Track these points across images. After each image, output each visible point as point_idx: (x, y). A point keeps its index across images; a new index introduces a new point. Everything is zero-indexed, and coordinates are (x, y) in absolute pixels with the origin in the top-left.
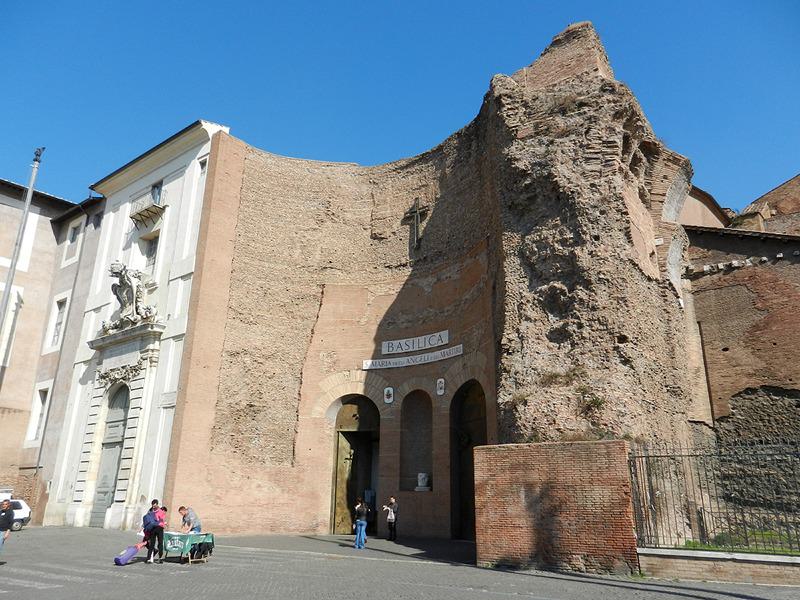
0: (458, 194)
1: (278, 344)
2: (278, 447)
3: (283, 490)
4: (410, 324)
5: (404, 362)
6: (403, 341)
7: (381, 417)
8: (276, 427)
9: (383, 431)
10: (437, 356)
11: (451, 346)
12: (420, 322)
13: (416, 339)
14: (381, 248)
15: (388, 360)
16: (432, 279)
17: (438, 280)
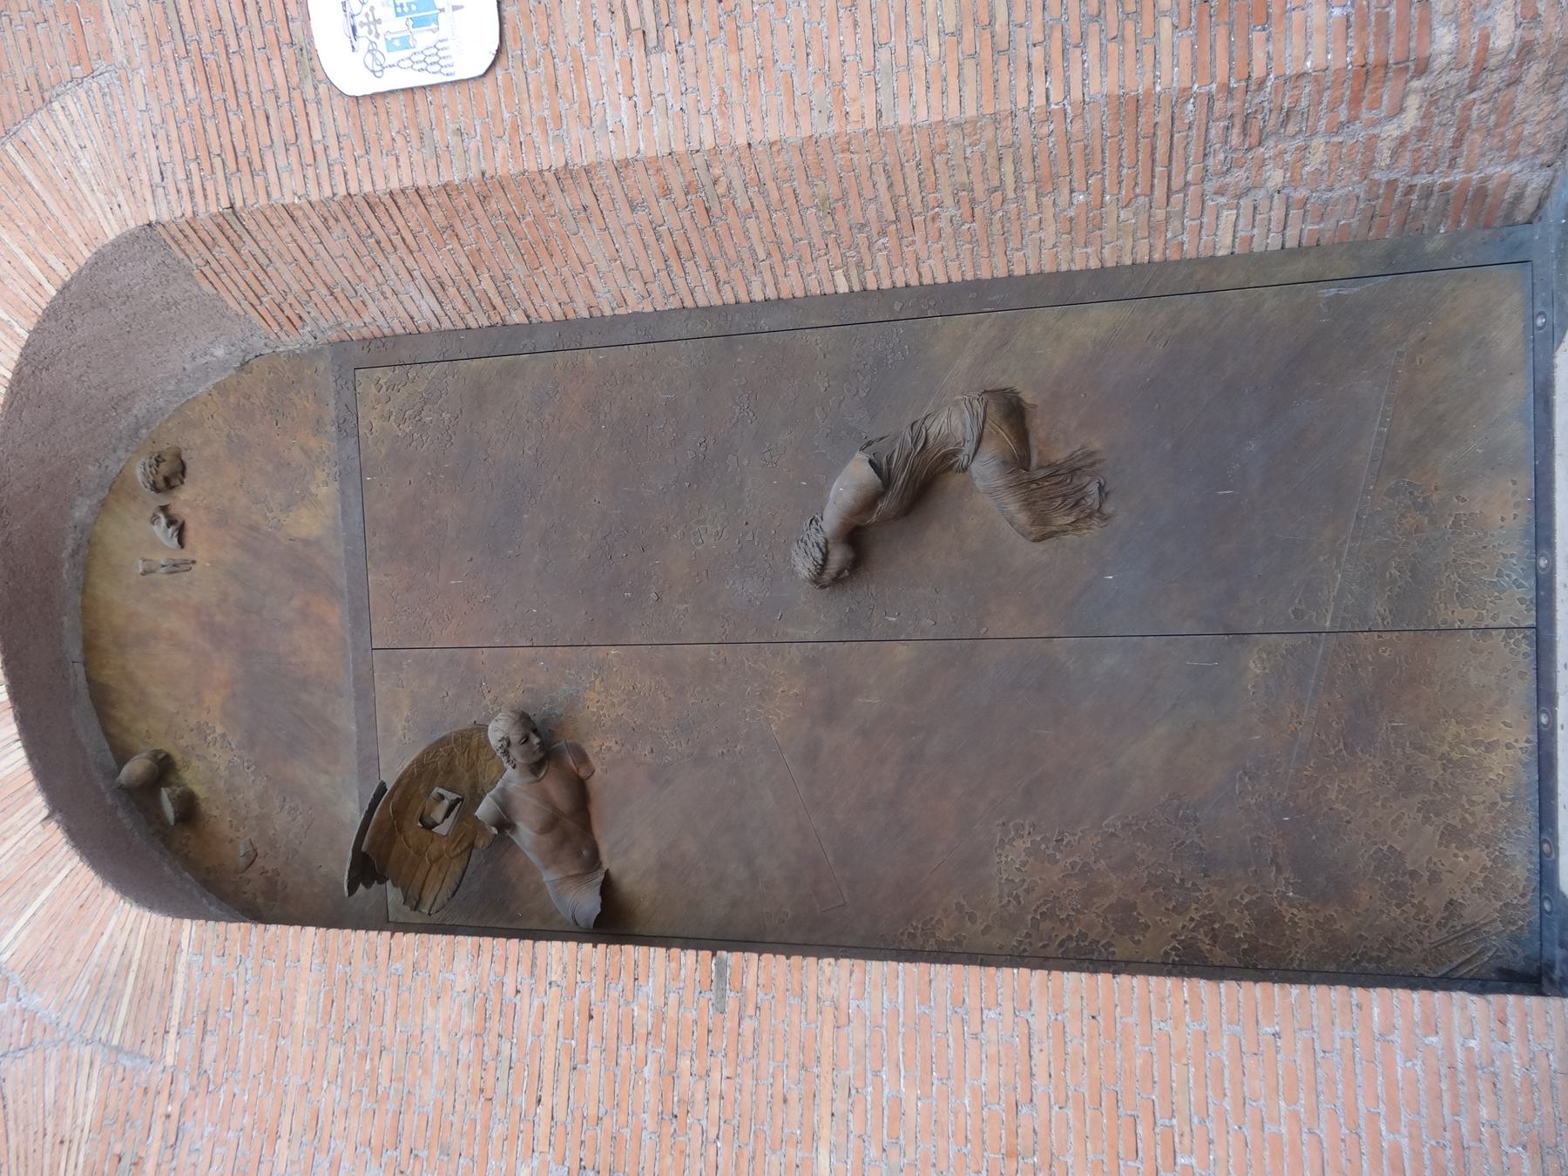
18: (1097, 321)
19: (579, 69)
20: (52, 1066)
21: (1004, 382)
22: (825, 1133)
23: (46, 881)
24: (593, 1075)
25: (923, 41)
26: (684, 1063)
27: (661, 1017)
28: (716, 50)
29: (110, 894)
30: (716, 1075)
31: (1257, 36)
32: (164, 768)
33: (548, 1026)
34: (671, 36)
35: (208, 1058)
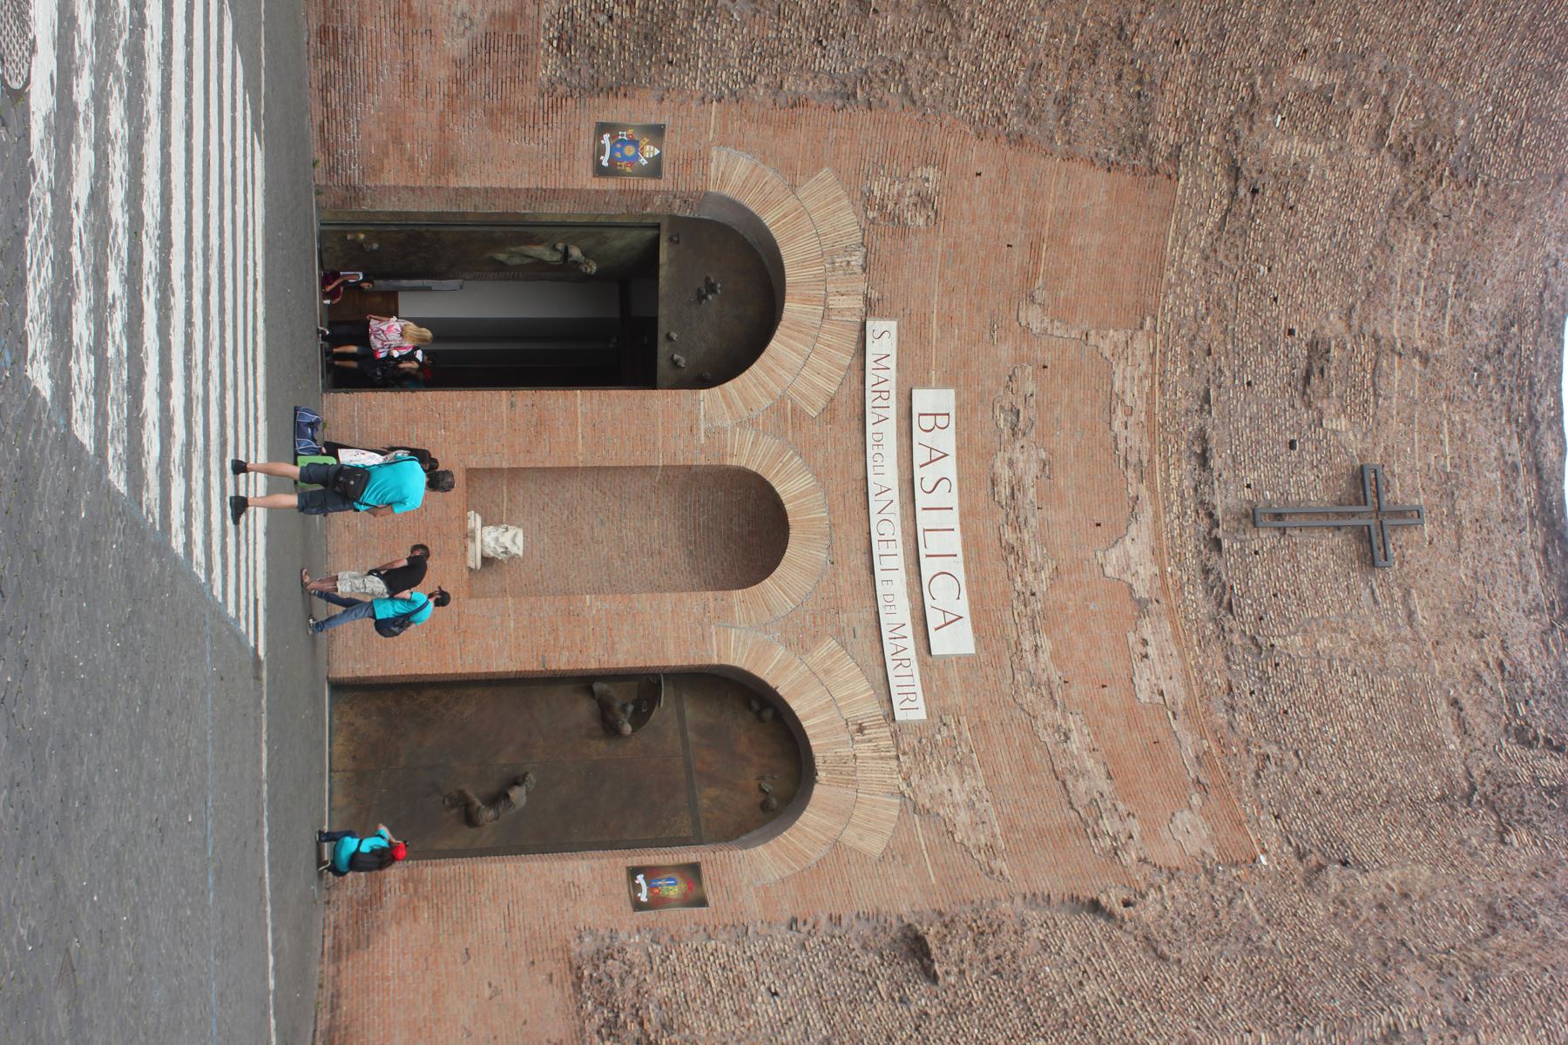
0: (1409, 686)
1: (982, 21)
2: (611, 32)
3: (458, 63)
4: (1004, 491)
5: (884, 474)
6: (949, 468)
7: (703, 393)
8: (681, 23)
9: (659, 401)
10: (896, 613)
11: (923, 665)
12: (1009, 536)
13: (953, 518)
14: (1274, 370)
15: (892, 413)
16: (1143, 579)
17: (1142, 606)
18: (445, 845)
19: (594, 879)
20: (754, 620)
21: (473, 831)
22: (512, 631)
23: (771, 670)
24: (578, 637)
25: (493, 881)
26: (552, 642)
27: (560, 653)
28: (552, 882)
29: (746, 668)
30: (543, 640)
31: (406, 876)
32: (760, 719)
33: (593, 647)
34: (567, 884)
35: (700, 628)
